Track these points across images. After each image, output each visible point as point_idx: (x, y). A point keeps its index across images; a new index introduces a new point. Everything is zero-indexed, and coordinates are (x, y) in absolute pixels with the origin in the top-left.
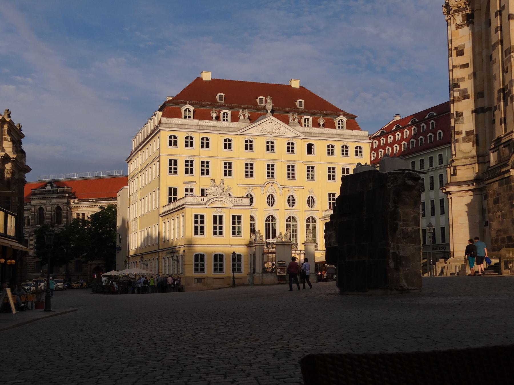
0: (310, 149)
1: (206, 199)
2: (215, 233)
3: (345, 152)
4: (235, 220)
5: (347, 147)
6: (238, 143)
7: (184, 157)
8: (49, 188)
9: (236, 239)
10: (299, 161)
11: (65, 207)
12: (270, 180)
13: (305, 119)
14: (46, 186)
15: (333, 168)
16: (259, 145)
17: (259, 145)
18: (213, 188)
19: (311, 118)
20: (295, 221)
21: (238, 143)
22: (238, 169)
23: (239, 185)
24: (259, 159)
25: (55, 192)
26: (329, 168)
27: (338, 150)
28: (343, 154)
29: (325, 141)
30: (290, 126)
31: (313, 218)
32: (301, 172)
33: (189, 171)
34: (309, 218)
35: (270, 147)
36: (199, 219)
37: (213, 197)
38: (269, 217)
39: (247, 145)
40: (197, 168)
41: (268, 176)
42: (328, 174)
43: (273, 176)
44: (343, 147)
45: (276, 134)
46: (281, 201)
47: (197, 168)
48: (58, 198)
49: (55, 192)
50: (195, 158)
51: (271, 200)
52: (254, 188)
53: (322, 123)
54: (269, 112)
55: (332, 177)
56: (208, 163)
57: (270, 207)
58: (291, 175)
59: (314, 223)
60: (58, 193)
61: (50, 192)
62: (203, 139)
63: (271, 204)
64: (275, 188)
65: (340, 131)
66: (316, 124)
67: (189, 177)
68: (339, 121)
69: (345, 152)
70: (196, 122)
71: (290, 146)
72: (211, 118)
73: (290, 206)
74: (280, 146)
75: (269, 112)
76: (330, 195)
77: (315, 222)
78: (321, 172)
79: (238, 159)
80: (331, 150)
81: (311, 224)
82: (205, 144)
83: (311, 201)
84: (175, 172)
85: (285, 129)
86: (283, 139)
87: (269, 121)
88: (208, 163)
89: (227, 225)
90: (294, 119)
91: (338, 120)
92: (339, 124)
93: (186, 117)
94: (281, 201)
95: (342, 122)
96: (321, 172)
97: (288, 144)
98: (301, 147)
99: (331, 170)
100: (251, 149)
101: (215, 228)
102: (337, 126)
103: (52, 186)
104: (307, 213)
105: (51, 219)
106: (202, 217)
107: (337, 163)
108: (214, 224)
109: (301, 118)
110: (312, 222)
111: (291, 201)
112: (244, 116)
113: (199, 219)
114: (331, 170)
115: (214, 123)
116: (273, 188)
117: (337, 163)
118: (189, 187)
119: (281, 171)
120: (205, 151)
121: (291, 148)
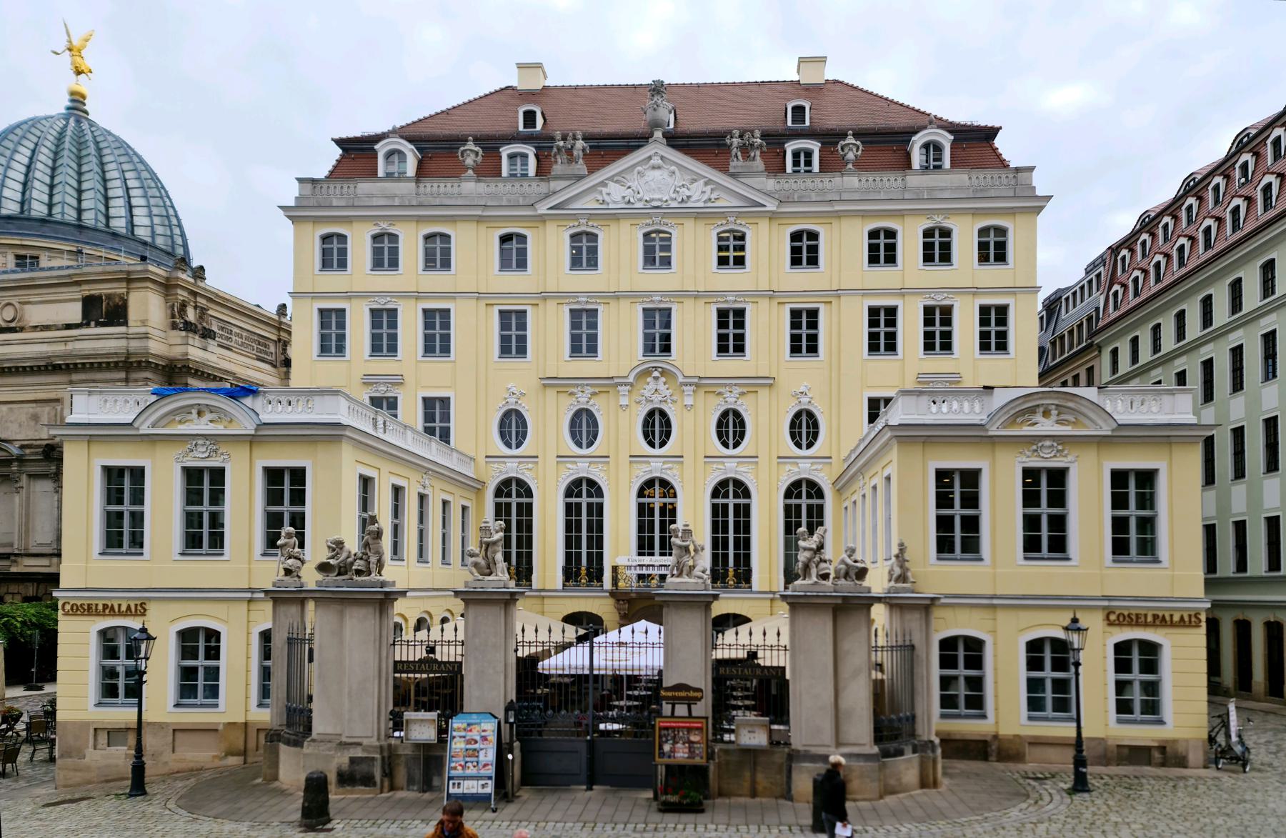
0: (804, 251)
3: (937, 248)
6: (550, 248)
10: (758, 294)
15: (891, 312)
16: (621, 248)
17: (621, 248)
19: (815, 146)
20: (747, 494)
21: (550, 248)
22: (549, 331)
24: (617, 296)
26: (874, 312)
27: (910, 245)
29: (857, 222)
30: (733, 176)
32: (767, 330)
33: (384, 343)
35: (656, 253)
40: (410, 330)
43: (666, 349)
46: (694, 425)
47: (410, 330)
51: (657, 427)
53: (851, 156)
67: (383, 366)
75: (658, 134)
80: (882, 249)
81: (804, 502)
82: (438, 254)
83: (804, 427)
85: (708, 188)
86: (701, 225)
96: (844, 328)
98: (768, 246)
102: (917, 158)
104: (788, 467)
111: (731, 428)
115: (470, 187)
117: (902, 292)
118: (381, 391)
119: (694, 333)
120: (437, 281)
121: (732, 253)
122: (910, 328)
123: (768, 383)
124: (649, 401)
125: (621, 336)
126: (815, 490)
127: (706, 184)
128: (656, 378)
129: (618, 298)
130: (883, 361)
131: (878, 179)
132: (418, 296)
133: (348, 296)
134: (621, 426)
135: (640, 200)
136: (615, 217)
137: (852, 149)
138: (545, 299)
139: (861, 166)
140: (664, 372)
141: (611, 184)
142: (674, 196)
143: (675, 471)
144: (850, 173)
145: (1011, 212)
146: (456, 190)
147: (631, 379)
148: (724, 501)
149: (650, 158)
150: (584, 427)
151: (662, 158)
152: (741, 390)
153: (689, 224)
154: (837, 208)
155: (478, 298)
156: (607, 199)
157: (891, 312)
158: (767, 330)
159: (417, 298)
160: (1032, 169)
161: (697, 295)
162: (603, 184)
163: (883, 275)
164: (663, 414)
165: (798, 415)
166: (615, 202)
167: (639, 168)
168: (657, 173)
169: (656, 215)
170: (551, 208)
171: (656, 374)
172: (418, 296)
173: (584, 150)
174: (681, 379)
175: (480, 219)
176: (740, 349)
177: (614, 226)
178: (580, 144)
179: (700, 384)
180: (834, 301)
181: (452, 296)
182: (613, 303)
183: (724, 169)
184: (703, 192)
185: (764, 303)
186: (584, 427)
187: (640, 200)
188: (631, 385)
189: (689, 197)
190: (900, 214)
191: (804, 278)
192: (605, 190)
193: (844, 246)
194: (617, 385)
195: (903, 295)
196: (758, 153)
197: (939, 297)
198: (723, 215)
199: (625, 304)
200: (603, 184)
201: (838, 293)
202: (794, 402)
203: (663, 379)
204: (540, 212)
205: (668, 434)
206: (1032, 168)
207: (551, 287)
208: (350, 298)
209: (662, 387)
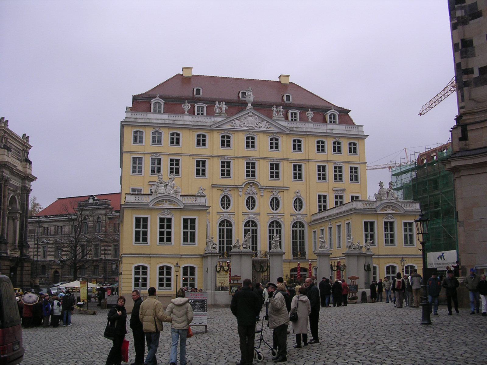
1: (151, 198)
2: (161, 240)
3: (337, 149)
4: (189, 224)
5: (339, 143)
6: (214, 139)
7: (150, 155)
8: (91, 201)
9: (188, 249)
10: (283, 159)
11: (104, 217)
12: (250, 179)
13: (292, 114)
14: (89, 199)
15: (324, 167)
16: (238, 142)
17: (238, 142)
18: (160, 185)
19: (298, 112)
21: (214, 139)
22: (214, 168)
23: (213, 186)
24: (238, 157)
25: (96, 204)
26: (319, 167)
28: (334, 151)
30: (273, 120)
31: (301, 223)
32: (286, 170)
34: (296, 223)
35: (250, 143)
36: (141, 223)
37: (159, 195)
38: (248, 222)
39: (223, 141)
41: (248, 175)
42: (317, 173)
43: (253, 176)
44: (334, 143)
45: (256, 129)
46: (263, 203)
48: (98, 209)
49: (96, 204)
50: (162, 156)
51: (251, 202)
52: (231, 189)
53: (310, 117)
54: (250, 105)
55: (322, 176)
56: (178, 161)
57: (250, 211)
58: (275, 175)
59: (302, 229)
60: (98, 205)
61: (92, 204)
62: (172, 134)
63: (251, 208)
64: (254, 189)
65: (330, 126)
66: (304, 119)
68: (330, 115)
69: (337, 149)
70: (165, 116)
71: (274, 142)
72: (182, 112)
73: (273, 209)
74: (262, 142)
75: (250, 105)
76: (320, 196)
77: (303, 227)
78: (310, 171)
79: (213, 156)
80: (321, 147)
81: (298, 229)
82: (175, 140)
83: (298, 203)
84: (140, 171)
85: (268, 124)
87: (250, 114)
88: (178, 161)
89: (177, 229)
90: (278, 112)
91: (329, 114)
92: (330, 118)
93: (155, 111)
94: (263, 203)
95: (334, 116)
96: (310, 171)
97: (271, 139)
98: (286, 143)
99: (322, 169)
100: (228, 145)
101: (162, 233)
102: (328, 120)
103: (93, 198)
105: (93, 228)
106: (145, 220)
107: (328, 162)
108: (184, 228)
109: (287, 112)
110: (300, 227)
111: (275, 203)
112: (220, 108)
113: (141, 223)
114: (322, 169)
116: (253, 189)
117: (328, 162)
119: (263, 171)
120: (175, 149)
121: (274, 145)
122: (330, 173)
123: (286, 189)
124: (248, 193)
125: (239, 171)
126: (302, 225)
127: (267, 122)
128: (251, 186)
129: (238, 158)
130: (322, 184)
131: (319, 125)
132: (169, 155)
133: (144, 153)
134: (238, 202)
135: (245, 126)
136: (237, 131)
137: (310, 114)
138: (213, 157)
139: (314, 120)
140: (254, 184)
141: (236, 120)
142: (256, 126)
143: (257, 218)
144: (310, 122)
145: (358, 139)
146: (182, 119)
147: (243, 186)
148: (273, 228)
149: (249, 113)
150: (226, 202)
151: (253, 113)
152: (279, 191)
153: (261, 135)
154: (307, 134)
155: (189, 156)
156: (234, 125)
157: (324, 167)
158: (286, 170)
159: (168, 155)
160: (362, 126)
161: (264, 159)
162: (233, 120)
163: (321, 156)
164: (253, 198)
165: (296, 200)
166: (237, 126)
167: (245, 116)
168: (251, 118)
169: (251, 132)
170: (215, 127)
171: (251, 184)
172: (169, 155)
173: (226, 108)
174: (260, 187)
175: (190, 129)
176: (277, 177)
177: (236, 134)
178: (224, 106)
179: (265, 188)
180: (307, 163)
181: (181, 155)
182: (236, 160)
183: (271, 117)
184: (266, 125)
185: (285, 162)
186: (226, 202)
187: (245, 126)
188: (243, 188)
189: (261, 126)
190: (326, 137)
191: (297, 155)
192: (234, 122)
193: (309, 146)
194: (238, 188)
195: (328, 162)
196: (282, 113)
197: (338, 164)
198: (272, 133)
199: (240, 160)
200: (233, 120)
201: (308, 161)
202: (295, 195)
203: (254, 186)
204: (212, 128)
205: (254, 205)
206: (362, 126)
207: (215, 153)
208: (144, 154)
209: (253, 189)
